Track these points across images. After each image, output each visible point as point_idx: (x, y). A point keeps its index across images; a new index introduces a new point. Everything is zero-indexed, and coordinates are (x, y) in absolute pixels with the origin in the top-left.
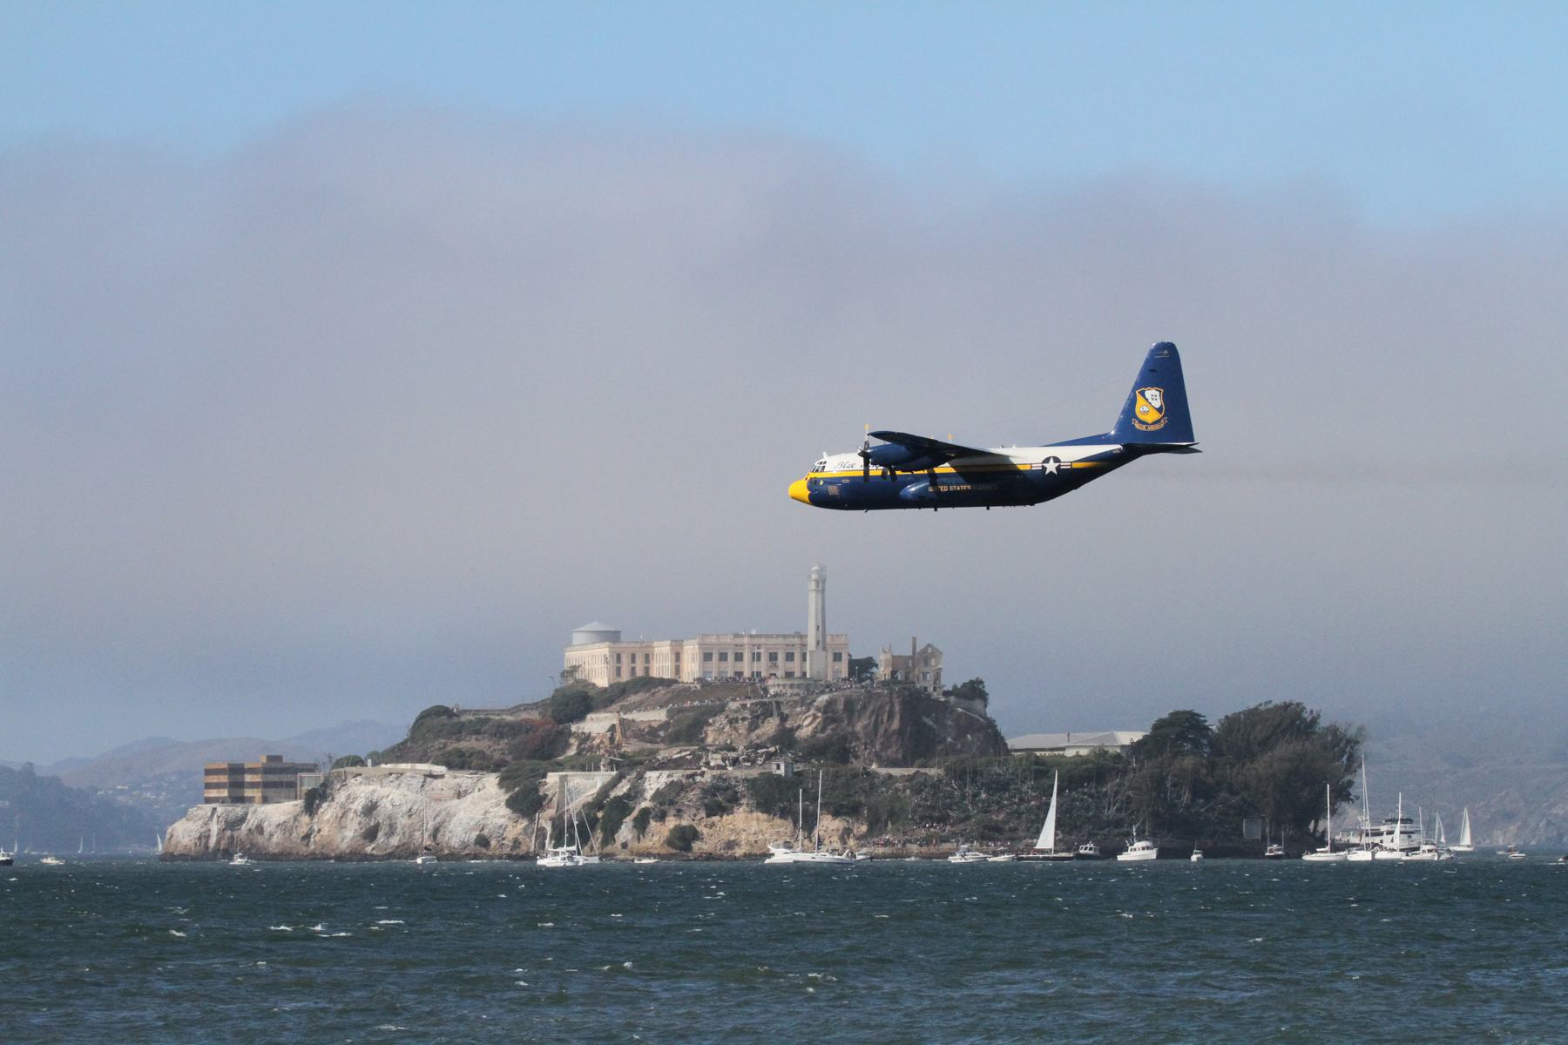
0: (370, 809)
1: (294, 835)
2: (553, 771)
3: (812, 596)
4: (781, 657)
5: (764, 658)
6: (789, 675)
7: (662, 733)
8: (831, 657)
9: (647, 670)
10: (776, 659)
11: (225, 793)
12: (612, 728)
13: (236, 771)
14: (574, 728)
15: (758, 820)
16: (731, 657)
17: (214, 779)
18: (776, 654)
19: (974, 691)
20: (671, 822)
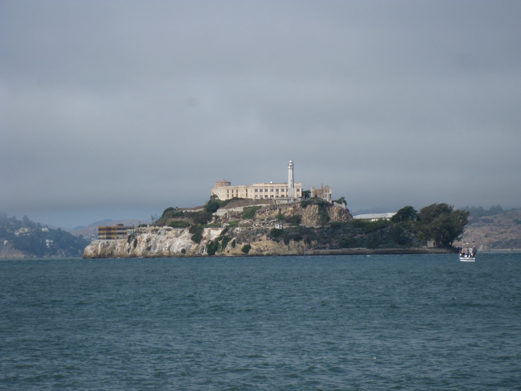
0: (148, 240)
1: (125, 249)
2: (206, 228)
3: (290, 172)
4: (280, 190)
5: (275, 190)
6: (283, 196)
7: (242, 215)
8: (296, 190)
9: (237, 195)
10: (278, 191)
11: (105, 236)
12: (226, 214)
13: (109, 229)
14: (214, 214)
15: (271, 243)
16: (264, 190)
17: (102, 232)
18: (278, 189)
19: (341, 201)
20: (243, 244)
